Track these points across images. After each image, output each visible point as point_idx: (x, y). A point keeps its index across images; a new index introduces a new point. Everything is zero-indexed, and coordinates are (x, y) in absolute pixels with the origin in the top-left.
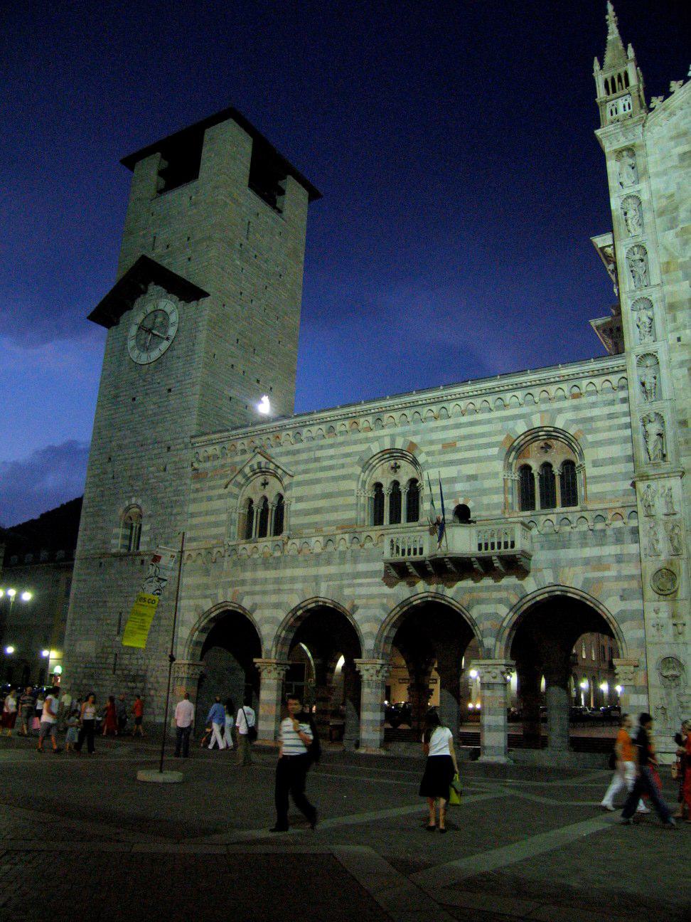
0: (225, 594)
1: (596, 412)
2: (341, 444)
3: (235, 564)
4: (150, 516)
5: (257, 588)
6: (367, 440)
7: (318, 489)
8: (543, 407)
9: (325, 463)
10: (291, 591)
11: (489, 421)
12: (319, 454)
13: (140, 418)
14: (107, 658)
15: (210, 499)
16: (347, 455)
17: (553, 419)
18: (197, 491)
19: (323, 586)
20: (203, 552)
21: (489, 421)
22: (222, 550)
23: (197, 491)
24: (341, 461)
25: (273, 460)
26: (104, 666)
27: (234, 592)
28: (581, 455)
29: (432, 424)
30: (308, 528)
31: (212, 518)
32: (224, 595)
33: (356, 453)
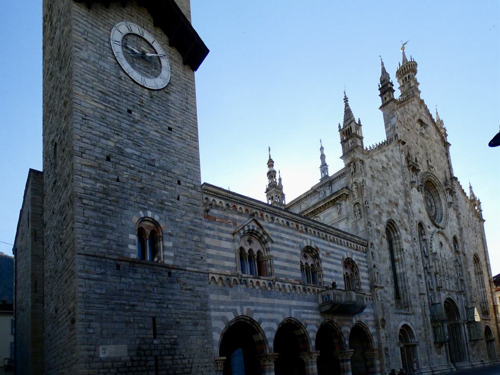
1: (361, 258)
2: (291, 234)
6: (301, 237)
7: (284, 256)
8: (350, 250)
9: (286, 242)
12: (283, 235)
14: (146, 361)
15: (220, 238)
16: (294, 242)
17: (352, 256)
18: (209, 229)
20: (224, 278)
23: (209, 229)
24: (292, 244)
25: (265, 229)
26: (144, 368)
29: (322, 241)
30: (282, 277)
31: (225, 254)
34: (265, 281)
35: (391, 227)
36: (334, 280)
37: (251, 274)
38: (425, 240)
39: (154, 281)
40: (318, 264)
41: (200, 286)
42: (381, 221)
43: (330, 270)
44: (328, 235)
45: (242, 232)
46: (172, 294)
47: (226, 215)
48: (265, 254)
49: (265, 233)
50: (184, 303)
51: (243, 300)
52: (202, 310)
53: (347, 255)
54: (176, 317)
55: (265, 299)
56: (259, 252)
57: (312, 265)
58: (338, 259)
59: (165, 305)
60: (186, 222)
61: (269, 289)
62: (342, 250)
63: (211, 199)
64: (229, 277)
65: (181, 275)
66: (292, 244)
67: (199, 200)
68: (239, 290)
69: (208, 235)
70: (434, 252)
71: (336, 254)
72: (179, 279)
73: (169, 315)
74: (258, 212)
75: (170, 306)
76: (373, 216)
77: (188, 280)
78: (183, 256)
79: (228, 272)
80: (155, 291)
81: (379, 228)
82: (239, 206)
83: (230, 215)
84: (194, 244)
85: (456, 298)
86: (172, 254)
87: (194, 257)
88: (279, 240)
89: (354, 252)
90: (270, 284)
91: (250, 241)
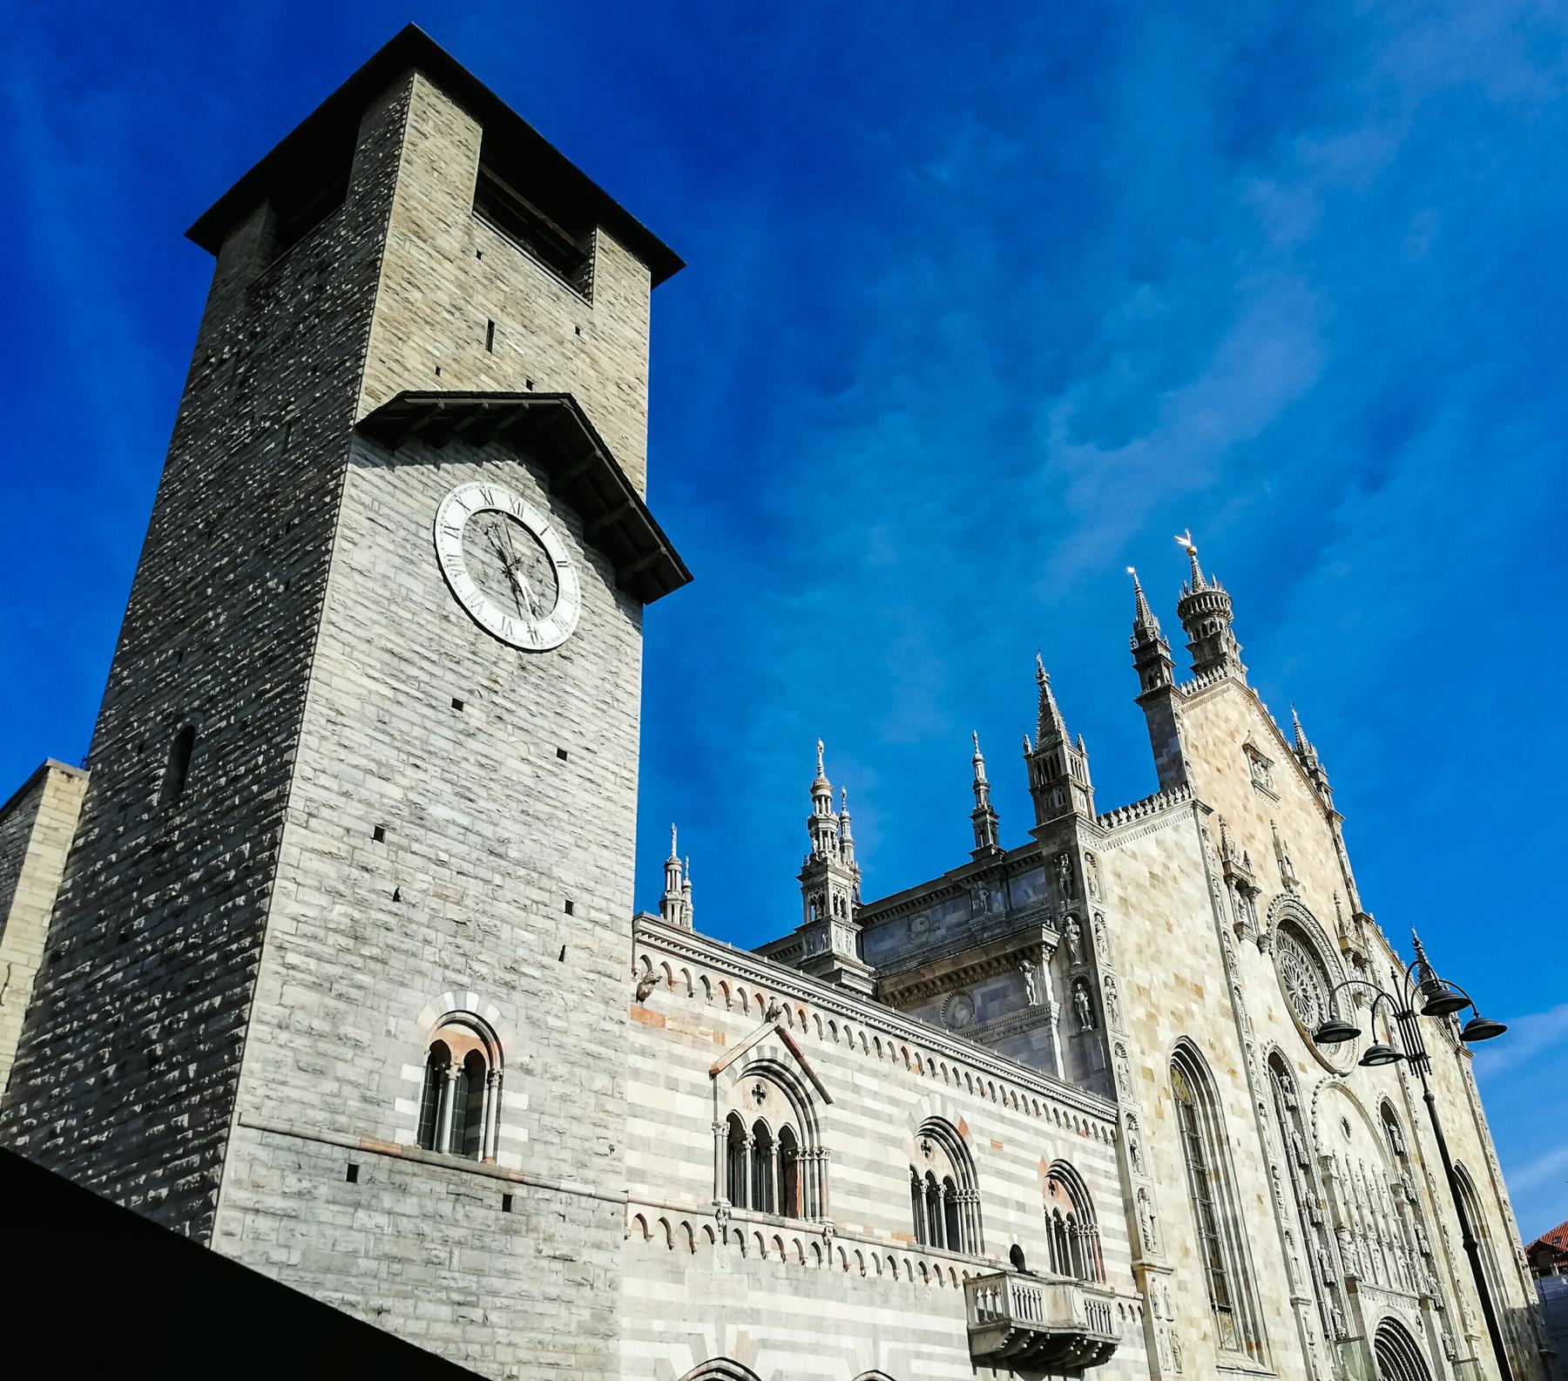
0: (720, 1340)
1: (1098, 1163)
3: (737, 1268)
4: (529, 1072)
5: (780, 1334)
6: (915, 1088)
7: (862, 1148)
8: (1063, 1132)
9: (869, 1103)
10: (838, 1352)
11: (1025, 1128)
12: (861, 1079)
13: (482, 772)
15: (672, 1085)
16: (894, 1102)
19: (885, 1347)
20: (674, 1219)
21: (1025, 1128)
22: (712, 1223)
23: (643, 1052)
24: (888, 1109)
25: (807, 1059)
27: (741, 1336)
28: (1088, 1213)
29: (976, 1099)
31: (682, 1137)
32: (723, 1343)
33: (908, 1105)
34: (801, 1236)
35: (1187, 1061)
36: (1015, 1236)
37: (757, 1206)
38: (1293, 1109)
39: (455, 1223)
40: (965, 1177)
41: (598, 1246)
42: (1154, 1042)
43: (1003, 1202)
44: (997, 1083)
45: (739, 1065)
46: (506, 1274)
47: (696, 1010)
48: (802, 1141)
49: (806, 1070)
50: (541, 1307)
51: (729, 1302)
52: (595, 1334)
53: (1055, 1150)
54: (509, 1359)
55: (797, 1299)
56: (786, 1133)
57: (947, 1180)
58: (1028, 1164)
59: (477, 1314)
60: (576, 1030)
61: (811, 1261)
62: (1038, 1132)
63: (657, 958)
64: (688, 1218)
65: (543, 1204)
66: (888, 1109)
67: (621, 963)
68: (716, 1262)
69: (636, 1073)
70: (1325, 1152)
71: (1021, 1145)
72: (534, 1220)
73: (488, 1349)
74: (791, 1002)
75: (494, 1317)
76: (1132, 1023)
77: (561, 1225)
78: (556, 1140)
79: (687, 1200)
80: (455, 1260)
81: (1150, 1063)
82: (735, 984)
83: (709, 1012)
84: (592, 1101)
85: (1413, 1322)
86: (521, 1134)
87: (587, 1145)
88: (850, 1096)
89: (1078, 1139)
90: (815, 1245)
91: (760, 1094)
